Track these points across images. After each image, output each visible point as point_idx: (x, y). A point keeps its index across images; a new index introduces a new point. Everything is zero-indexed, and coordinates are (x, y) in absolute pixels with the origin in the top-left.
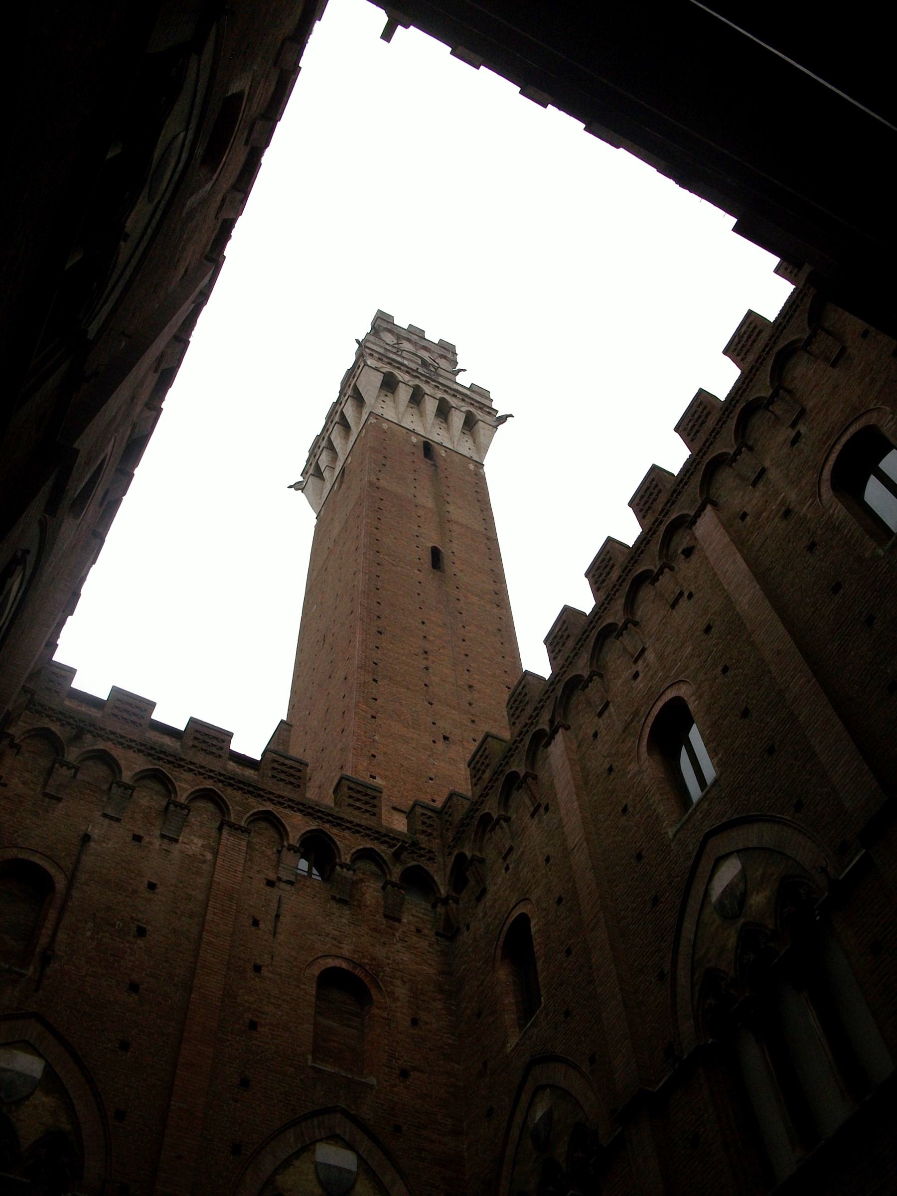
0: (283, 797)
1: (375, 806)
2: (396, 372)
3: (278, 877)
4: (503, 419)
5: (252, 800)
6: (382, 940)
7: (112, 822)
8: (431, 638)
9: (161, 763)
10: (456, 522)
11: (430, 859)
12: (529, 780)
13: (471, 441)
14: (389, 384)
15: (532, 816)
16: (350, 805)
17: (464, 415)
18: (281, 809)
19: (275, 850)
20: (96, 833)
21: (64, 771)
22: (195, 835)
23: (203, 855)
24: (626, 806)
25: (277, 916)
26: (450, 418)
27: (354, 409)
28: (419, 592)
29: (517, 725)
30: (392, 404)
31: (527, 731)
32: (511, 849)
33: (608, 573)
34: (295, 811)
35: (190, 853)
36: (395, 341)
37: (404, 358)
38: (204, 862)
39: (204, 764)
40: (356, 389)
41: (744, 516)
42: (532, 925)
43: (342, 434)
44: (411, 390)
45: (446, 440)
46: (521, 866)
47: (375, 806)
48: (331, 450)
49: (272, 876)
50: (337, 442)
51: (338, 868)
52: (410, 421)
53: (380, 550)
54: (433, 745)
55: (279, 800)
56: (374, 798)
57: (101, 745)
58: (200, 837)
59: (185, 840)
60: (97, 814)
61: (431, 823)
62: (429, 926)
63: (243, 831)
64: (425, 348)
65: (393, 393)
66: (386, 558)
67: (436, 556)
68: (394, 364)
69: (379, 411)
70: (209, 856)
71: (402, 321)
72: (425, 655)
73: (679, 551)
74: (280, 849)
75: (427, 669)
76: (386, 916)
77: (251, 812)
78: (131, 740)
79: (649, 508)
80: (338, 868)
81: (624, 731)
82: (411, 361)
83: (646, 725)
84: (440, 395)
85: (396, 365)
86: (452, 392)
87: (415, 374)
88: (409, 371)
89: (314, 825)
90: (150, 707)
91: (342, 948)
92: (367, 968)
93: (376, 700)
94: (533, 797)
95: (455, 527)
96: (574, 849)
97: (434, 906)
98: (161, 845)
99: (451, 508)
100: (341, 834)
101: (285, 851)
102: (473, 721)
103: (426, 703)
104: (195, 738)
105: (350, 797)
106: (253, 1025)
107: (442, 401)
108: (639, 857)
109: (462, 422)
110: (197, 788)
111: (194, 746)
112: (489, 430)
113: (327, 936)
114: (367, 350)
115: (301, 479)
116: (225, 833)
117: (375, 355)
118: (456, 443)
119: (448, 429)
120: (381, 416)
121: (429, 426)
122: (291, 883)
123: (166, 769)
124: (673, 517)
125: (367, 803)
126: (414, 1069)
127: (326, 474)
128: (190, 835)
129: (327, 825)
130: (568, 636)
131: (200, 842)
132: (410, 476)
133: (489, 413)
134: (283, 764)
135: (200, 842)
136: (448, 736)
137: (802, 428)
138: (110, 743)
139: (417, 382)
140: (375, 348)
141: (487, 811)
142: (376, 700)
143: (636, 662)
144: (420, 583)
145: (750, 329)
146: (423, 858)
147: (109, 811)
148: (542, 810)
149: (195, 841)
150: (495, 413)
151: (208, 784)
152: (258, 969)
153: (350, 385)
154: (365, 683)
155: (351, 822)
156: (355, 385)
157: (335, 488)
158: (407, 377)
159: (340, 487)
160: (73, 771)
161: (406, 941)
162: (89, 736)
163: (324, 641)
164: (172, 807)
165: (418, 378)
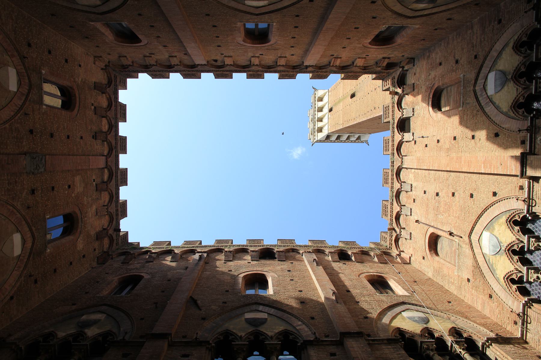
2: (316, 129)
6: (420, 89)
11: (394, 78)
12: (331, 65)
14: (320, 130)
15: (340, 58)
25: (423, 137)
32: (359, 58)
40: (326, 139)
43: (342, 137)
49: (413, 142)
51: (404, 117)
55: (393, 145)
58: (409, 175)
60: (412, 217)
63: (403, 159)
67: (353, 96)
76: (414, 90)
81: (278, 50)
92: (429, 93)
97: (407, 70)
126: (454, 57)
131: (410, 175)
137: (148, 55)
139: (316, 121)
143: (258, 57)
148: (335, 56)
158: (316, 125)
160: (401, 230)
164: (402, 189)
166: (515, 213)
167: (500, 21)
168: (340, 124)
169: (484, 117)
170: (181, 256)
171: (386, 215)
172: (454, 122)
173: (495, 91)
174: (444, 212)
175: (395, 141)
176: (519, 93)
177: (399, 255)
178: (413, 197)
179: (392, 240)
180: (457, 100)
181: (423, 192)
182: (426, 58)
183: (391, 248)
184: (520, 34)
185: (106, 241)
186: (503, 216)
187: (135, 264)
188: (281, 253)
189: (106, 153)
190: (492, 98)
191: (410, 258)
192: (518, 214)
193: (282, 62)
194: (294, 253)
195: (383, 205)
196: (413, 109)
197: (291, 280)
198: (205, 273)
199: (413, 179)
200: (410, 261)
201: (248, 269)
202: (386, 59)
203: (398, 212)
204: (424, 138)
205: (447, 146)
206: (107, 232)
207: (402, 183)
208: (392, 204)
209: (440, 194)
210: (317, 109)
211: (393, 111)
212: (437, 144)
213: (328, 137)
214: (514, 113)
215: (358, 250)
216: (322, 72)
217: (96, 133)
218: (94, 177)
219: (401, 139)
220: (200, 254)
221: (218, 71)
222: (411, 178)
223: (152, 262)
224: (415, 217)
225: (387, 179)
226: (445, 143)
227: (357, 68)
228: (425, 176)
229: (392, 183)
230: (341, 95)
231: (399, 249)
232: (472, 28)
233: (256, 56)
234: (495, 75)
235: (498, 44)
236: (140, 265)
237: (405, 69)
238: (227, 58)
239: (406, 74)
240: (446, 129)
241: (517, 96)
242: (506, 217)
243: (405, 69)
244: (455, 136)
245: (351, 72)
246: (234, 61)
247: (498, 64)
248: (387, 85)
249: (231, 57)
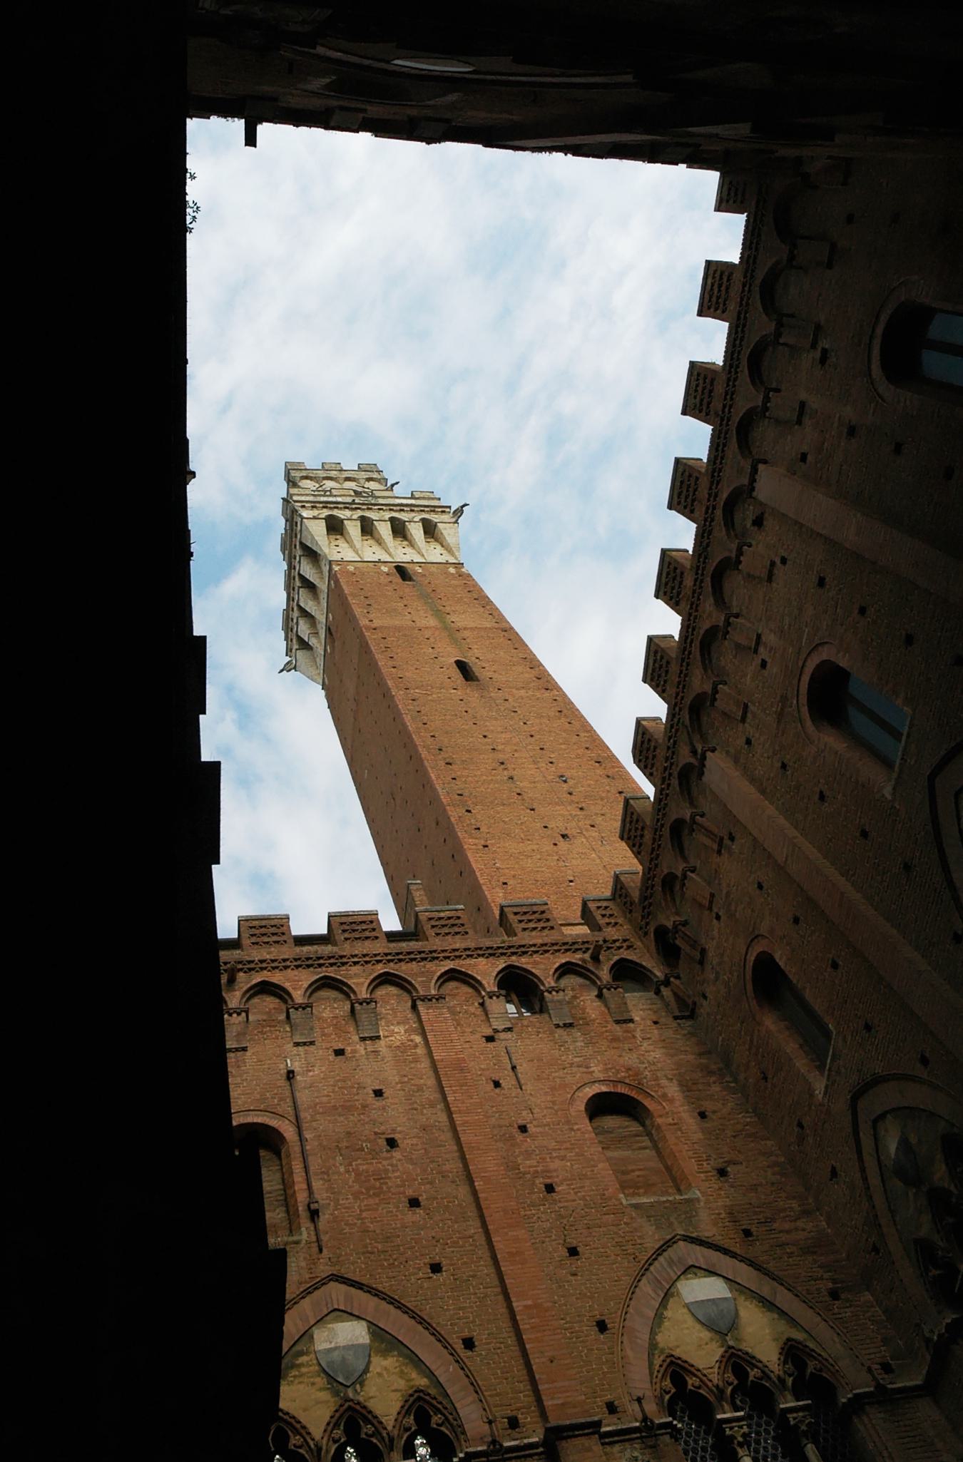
0: (457, 950)
1: (548, 920)
2: (335, 512)
3: (494, 1029)
4: (459, 512)
5: (430, 966)
6: (626, 1046)
7: (306, 1048)
8: (500, 748)
9: (324, 969)
10: (465, 629)
11: (629, 947)
13: (439, 547)
14: (335, 527)
15: (719, 852)
16: (524, 929)
17: (420, 524)
18: (462, 962)
19: (476, 1004)
20: (296, 1066)
22: (392, 1025)
23: (412, 1041)
24: (821, 792)
25: (514, 1068)
27: (311, 566)
28: (465, 709)
29: (655, 773)
30: (346, 545)
31: (670, 774)
32: (712, 895)
33: (681, 583)
34: (476, 958)
35: (398, 1044)
36: (317, 485)
37: (335, 496)
38: (416, 1046)
39: (365, 952)
41: (803, 458)
42: (778, 960)
44: (358, 523)
45: (415, 556)
46: (733, 908)
47: (548, 920)
48: (306, 616)
49: (489, 1032)
50: (310, 606)
51: (546, 994)
52: (371, 552)
53: (409, 685)
54: (555, 848)
55: (455, 954)
56: (543, 912)
57: (257, 978)
58: (399, 1023)
59: (386, 1034)
61: (611, 913)
62: (663, 1014)
64: (348, 479)
66: (417, 691)
68: (329, 505)
69: (337, 557)
71: (312, 463)
72: (502, 766)
73: (748, 526)
74: (481, 1001)
75: (511, 778)
76: (618, 1022)
77: (436, 978)
78: (284, 960)
79: (693, 501)
80: (546, 994)
82: (344, 495)
83: (800, 705)
84: (387, 515)
85: (332, 506)
86: (398, 508)
87: (354, 506)
88: (347, 506)
89: (501, 963)
90: (284, 921)
91: (594, 1072)
92: (627, 1081)
93: (479, 829)
94: (709, 833)
95: (466, 634)
96: (786, 860)
98: (365, 1049)
100: (532, 960)
101: (488, 1001)
102: (581, 809)
103: (529, 811)
104: (344, 931)
105: (520, 921)
106: (550, 1188)
107: (392, 520)
108: (864, 834)
109: (422, 532)
110: (372, 977)
111: (346, 939)
112: (450, 528)
113: (571, 1067)
114: (297, 504)
115: (288, 659)
116: (421, 1007)
117: (307, 505)
118: (425, 554)
119: (412, 544)
120: (342, 560)
122: (509, 1029)
123: (331, 972)
124: (725, 495)
125: (539, 920)
127: (313, 642)
128: (388, 1026)
129: (514, 958)
130: (668, 663)
131: (401, 1029)
132: (399, 604)
134: (440, 919)
136: (566, 833)
138: (265, 972)
140: (303, 498)
141: (666, 871)
142: (479, 829)
144: (461, 700)
145: (718, 278)
146: (621, 950)
147: (298, 1039)
148: (727, 842)
149: (396, 1030)
150: (448, 510)
151: (380, 969)
152: (523, 1129)
153: (295, 546)
154: (460, 817)
155: (535, 945)
156: (301, 543)
157: (329, 650)
158: (348, 513)
159: (333, 648)
160: (244, 1014)
161: (649, 1038)
162: (241, 974)
163: (394, 799)
165: (359, 508)
166: (445, 1412)
167: (834, 1295)
168: (371, 616)
169: (627, 1280)
173: (692, 1303)
174: (358, 1174)
175: (473, 961)
176: (705, 1375)
182: (702, 1061)
184: (820, 1355)
186: (426, 1377)
190: (672, 1295)
192: (447, 1419)
196: (571, 1025)
204: (511, 1073)
209: (397, 1154)
210: (398, 519)
211: (543, 949)
212: (516, 1126)
213: (312, 554)
214: (661, 1366)
226: (528, 1154)
228: (420, 1089)
232: (806, 1213)
234: (726, 1299)
235: (789, 1295)
237: (662, 988)
239: (646, 989)
241: (699, 1370)
242: (428, 1387)
243: (662, 988)
247: (747, 1303)
248: (604, 916)
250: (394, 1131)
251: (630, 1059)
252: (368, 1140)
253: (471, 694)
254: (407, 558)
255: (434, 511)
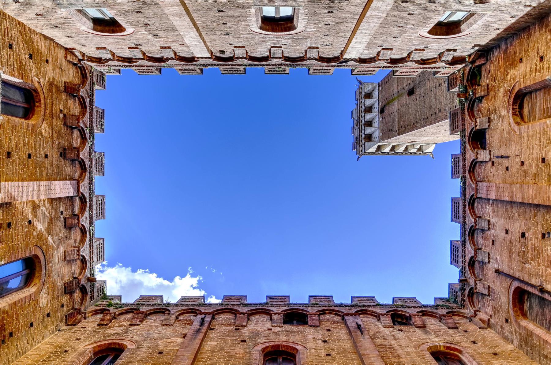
1: (455, 113)
2: (363, 137)
14: (369, 138)
15: (391, 49)
20: (496, 266)
21: (478, 286)
26: (369, 106)
32: (416, 50)
38: (493, 203)
49: (490, 163)
51: (478, 128)
55: (464, 165)
58: (486, 208)
60: (491, 266)
65: (371, 135)
67: (411, 92)
69: (378, 138)
70: (491, 201)
84: (363, 114)
92: (508, 97)
95: (399, 89)
99: (394, 92)
100: (467, 130)
101: (479, 160)
105: (455, 128)
121: (375, 114)
126: (538, 53)
127: (418, 147)
131: (488, 207)
133: (361, 88)
135: (488, 207)
139: (363, 126)
147: (486, 260)
148: (384, 47)
158: (363, 131)
160: (477, 282)
170: (177, 318)
171: (457, 261)
172: (542, 138)
177: (475, 315)
178: (492, 237)
179: (464, 295)
180: (544, 109)
181: (505, 231)
183: (464, 306)
185: (77, 294)
187: (116, 327)
188: (313, 316)
189: (77, 175)
191: (489, 320)
193: (313, 53)
194: (332, 316)
195: (453, 248)
196: (489, 118)
197: (327, 355)
198: (209, 343)
199: (491, 213)
200: (489, 324)
201: (269, 339)
202: (451, 52)
203: (472, 257)
205: (533, 170)
206: (79, 282)
207: (477, 219)
208: (464, 245)
209: (527, 235)
211: (463, 120)
215: (418, 310)
216: (367, 67)
217: (65, 149)
218: (62, 209)
219: (473, 158)
220: (203, 316)
221: (226, 65)
222: (488, 212)
223: (138, 325)
224: (493, 265)
225: (457, 212)
226: (531, 166)
227: (414, 62)
229: (464, 218)
230: (395, 90)
231: (474, 307)
233: (278, 46)
236: (122, 328)
238: (237, 49)
240: (531, 147)
244: (544, 157)
245: (406, 67)
246: (247, 52)
249: (244, 47)
250: (519, 232)
251: (502, 90)
252: (521, 247)
253: (419, 91)
254: (377, 107)
255: (361, 92)
